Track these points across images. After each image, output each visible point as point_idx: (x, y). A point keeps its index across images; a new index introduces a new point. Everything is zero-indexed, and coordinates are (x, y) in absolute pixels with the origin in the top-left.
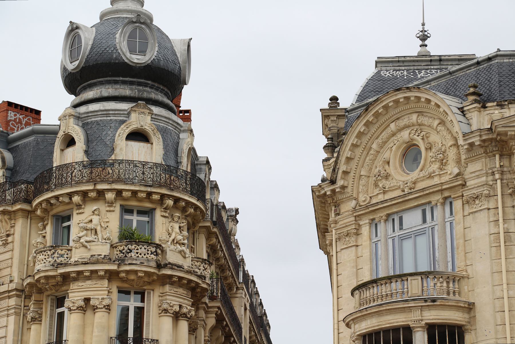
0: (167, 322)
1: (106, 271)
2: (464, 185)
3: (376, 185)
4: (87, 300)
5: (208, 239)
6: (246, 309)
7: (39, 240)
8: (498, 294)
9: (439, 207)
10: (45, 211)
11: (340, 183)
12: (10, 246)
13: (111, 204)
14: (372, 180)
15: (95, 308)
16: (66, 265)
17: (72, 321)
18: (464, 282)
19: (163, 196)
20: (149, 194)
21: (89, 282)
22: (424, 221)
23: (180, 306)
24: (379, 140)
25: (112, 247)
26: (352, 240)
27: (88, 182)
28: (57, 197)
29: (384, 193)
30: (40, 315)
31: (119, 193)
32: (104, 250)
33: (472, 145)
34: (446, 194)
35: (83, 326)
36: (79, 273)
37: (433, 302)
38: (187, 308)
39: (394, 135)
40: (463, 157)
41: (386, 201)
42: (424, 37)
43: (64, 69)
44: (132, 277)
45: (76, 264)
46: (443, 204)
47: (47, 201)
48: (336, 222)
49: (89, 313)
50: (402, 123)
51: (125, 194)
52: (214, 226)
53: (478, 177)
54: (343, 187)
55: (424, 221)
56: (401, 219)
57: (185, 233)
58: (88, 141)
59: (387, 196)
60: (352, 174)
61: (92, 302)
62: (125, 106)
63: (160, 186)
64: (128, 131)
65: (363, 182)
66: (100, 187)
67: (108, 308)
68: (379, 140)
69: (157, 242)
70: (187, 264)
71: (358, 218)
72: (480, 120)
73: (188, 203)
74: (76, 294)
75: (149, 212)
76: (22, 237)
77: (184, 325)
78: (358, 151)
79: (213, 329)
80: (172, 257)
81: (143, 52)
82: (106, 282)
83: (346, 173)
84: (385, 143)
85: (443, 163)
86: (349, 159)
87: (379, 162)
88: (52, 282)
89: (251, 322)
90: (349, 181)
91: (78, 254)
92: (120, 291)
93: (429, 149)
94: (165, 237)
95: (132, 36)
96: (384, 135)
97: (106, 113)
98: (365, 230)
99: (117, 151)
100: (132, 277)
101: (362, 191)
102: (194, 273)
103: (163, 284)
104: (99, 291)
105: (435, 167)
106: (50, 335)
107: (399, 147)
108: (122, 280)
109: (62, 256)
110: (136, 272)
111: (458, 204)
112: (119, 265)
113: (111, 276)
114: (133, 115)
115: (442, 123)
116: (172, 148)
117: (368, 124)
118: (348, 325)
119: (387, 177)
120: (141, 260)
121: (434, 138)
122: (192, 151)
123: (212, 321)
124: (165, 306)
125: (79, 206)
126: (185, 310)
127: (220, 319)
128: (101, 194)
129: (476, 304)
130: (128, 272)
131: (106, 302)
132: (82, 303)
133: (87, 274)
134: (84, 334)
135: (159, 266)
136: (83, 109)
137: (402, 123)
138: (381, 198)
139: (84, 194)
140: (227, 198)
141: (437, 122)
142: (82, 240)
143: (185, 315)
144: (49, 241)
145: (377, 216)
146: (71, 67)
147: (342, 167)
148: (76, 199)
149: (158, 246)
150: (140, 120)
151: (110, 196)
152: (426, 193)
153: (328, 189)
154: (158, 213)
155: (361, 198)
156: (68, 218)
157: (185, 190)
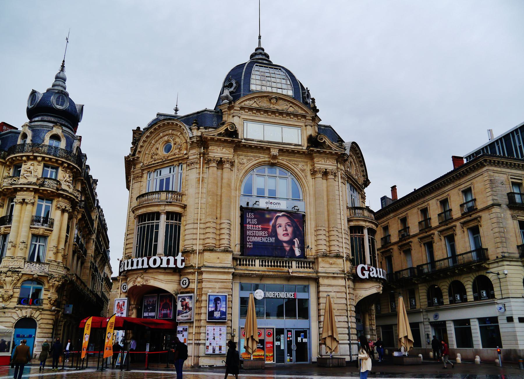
0: (59, 212)
1: (34, 189)
2: (187, 158)
3: (152, 158)
4: (24, 200)
5: (82, 185)
6: (96, 217)
7: (7, 174)
8: (197, 202)
9: (177, 167)
10: (11, 163)
11: (137, 156)
13: (39, 162)
14: (150, 156)
15: (27, 203)
16: (16, 184)
17: (17, 208)
18: (184, 197)
19: (63, 162)
20: (57, 160)
21: (25, 192)
22: (170, 172)
23: (66, 207)
24: (155, 140)
25: (38, 179)
26: (139, 179)
27: (30, 152)
28: (16, 157)
29: (155, 160)
30: (3, 205)
31: (43, 158)
32: (34, 180)
33: (193, 142)
34: (180, 162)
35: (21, 210)
36: (22, 188)
37: (170, 204)
38: (68, 208)
39: (161, 138)
40: (189, 147)
41: (155, 164)
42: (176, 110)
43: (28, 108)
44: (45, 192)
45: (21, 184)
46: (178, 166)
47: (12, 158)
48: (133, 172)
49: (24, 205)
50: (165, 133)
52: (86, 183)
53: (194, 155)
54: (138, 158)
55: (170, 172)
56: (161, 171)
57: (71, 179)
58: (33, 137)
59: (156, 162)
60: (142, 153)
61: (26, 201)
62: (51, 125)
63: (62, 158)
64: (51, 134)
65: (147, 156)
66: (35, 154)
67: (33, 204)
68: (155, 140)
69: (58, 179)
70: (71, 191)
71: (143, 170)
72: (197, 133)
74: (19, 197)
75: (57, 168)
77: (66, 215)
78: (146, 144)
79: (80, 220)
80: (64, 187)
81: (62, 105)
82: (33, 193)
83: (140, 152)
84: (157, 141)
85: (180, 150)
86: (142, 147)
87: (154, 148)
88: (10, 191)
89: (98, 224)
90: (141, 156)
91: (22, 181)
92: (40, 198)
93: (175, 144)
94: (62, 178)
95: (58, 98)
96: (157, 138)
97: (42, 126)
98: (145, 175)
99: (45, 141)
100: (45, 192)
101: (145, 159)
102: (74, 195)
103: (59, 197)
104: (29, 197)
105: (177, 151)
106: (7, 213)
107: (163, 143)
109: (15, 181)
110: (47, 190)
111: (184, 166)
112: (40, 187)
113: (36, 191)
114: (54, 128)
115: (182, 134)
116: (69, 144)
117: (151, 133)
118: (133, 212)
119: (156, 155)
120: (50, 186)
121: (177, 140)
122: (78, 149)
123: (80, 217)
124: (58, 206)
125: (25, 162)
126: (67, 209)
127: (83, 216)
129: (188, 207)
130: (43, 190)
131: (32, 201)
132: (21, 201)
133: (25, 189)
134: (21, 213)
135: (58, 189)
136: (33, 124)
137: (165, 133)
138: (153, 162)
139: (28, 157)
140: (93, 173)
141: (179, 133)
142: (25, 175)
143: (67, 211)
144: (11, 175)
145: (151, 170)
146: (30, 107)
147: (139, 149)
148: (24, 158)
149: (58, 181)
150: (57, 131)
151: (39, 159)
152: (172, 161)
153: (131, 158)
154: (60, 169)
155: (145, 162)
156: (21, 167)
157: (74, 163)
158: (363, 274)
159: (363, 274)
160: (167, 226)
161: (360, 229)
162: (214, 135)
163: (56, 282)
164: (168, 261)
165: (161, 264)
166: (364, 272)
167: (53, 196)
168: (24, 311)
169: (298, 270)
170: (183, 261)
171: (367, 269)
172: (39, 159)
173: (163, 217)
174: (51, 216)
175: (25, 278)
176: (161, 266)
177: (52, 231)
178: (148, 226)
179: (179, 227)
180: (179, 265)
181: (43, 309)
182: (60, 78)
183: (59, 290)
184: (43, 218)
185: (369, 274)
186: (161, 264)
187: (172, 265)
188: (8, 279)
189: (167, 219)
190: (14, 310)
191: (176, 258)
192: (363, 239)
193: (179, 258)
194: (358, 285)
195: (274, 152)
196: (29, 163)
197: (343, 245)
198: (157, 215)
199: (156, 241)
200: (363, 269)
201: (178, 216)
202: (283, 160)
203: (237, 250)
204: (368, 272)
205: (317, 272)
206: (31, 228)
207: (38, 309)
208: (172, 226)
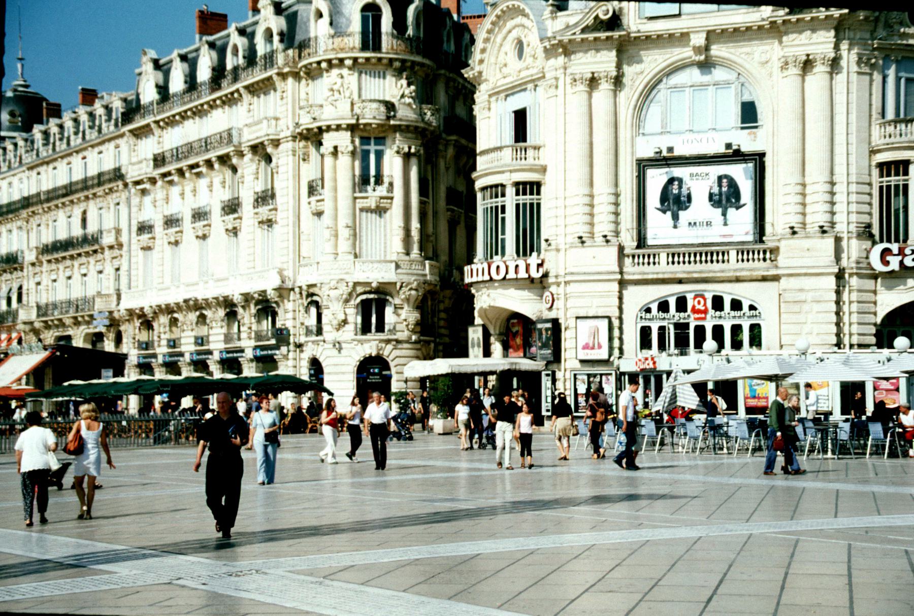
0: (398, 161)
12: (285, 100)
13: (350, 69)
19: (391, 60)
51: (360, 60)
73: (413, 62)
76: (293, 94)
82: (349, 133)
86: (483, 51)
87: (502, 54)
92: (362, 138)
103: (395, 132)
108: (362, 130)
110: (370, 124)
113: (352, 128)
128: (341, 60)
139: (329, 61)
151: (348, 62)
158: (887, 263)
159: (887, 263)
160: (518, 206)
162: (574, 34)
163: (413, 292)
165: (507, 273)
166: (888, 258)
167: (384, 132)
168: (366, 346)
171: (896, 251)
172: (348, 62)
173: (510, 191)
174: (386, 171)
175: (360, 289)
176: (508, 277)
177: (392, 198)
178: (492, 208)
179: (539, 205)
180: (535, 274)
181: (398, 341)
183: (421, 305)
184: (375, 176)
185: (901, 263)
186: (507, 273)
187: (523, 274)
188: (334, 293)
189: (517, 194)
190: (352, 345)
191: (528, 262)
193: (533, 260)
195: (698, 40)
196: (335, 72)
198: (497, 190)
199: (503, 233)
200: (886, 252)
201: (534, 187)
202: (717, 50)
204: (900, 258)
205: (777, 267)
206: (355, 198)
207: (388, 341)
208: (525, 205)
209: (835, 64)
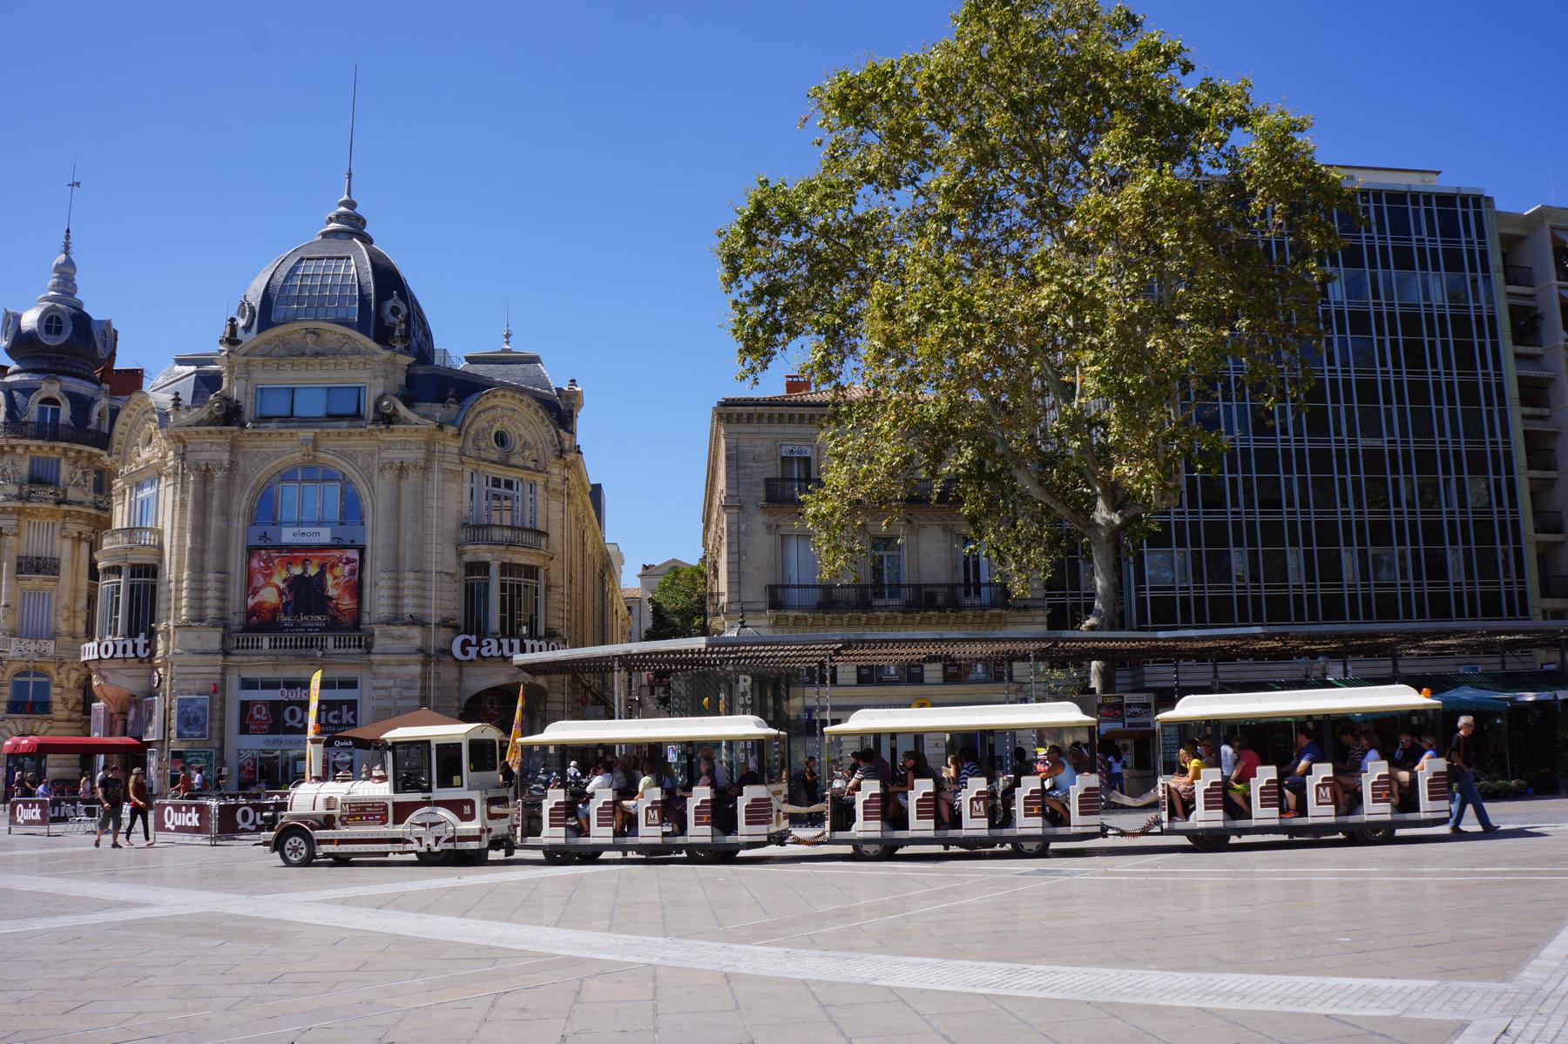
0: (67, 544)
31: (27, 447)
128: (13, 447)
151: (19, 451)
158: (465, 653)
159: (465, 653)
160: (132, 587)
161: (484, 567)
164: (125, 647)
169: (337, 651)
170: (146, 646)
179: (154, 588)
182: (66, 275)
185: (479, 653)
192: (487, 585)
194: (467, 670)
197: (444, 600)
200: (466, 643)
203: (236, 620)
209: (426, 469)
